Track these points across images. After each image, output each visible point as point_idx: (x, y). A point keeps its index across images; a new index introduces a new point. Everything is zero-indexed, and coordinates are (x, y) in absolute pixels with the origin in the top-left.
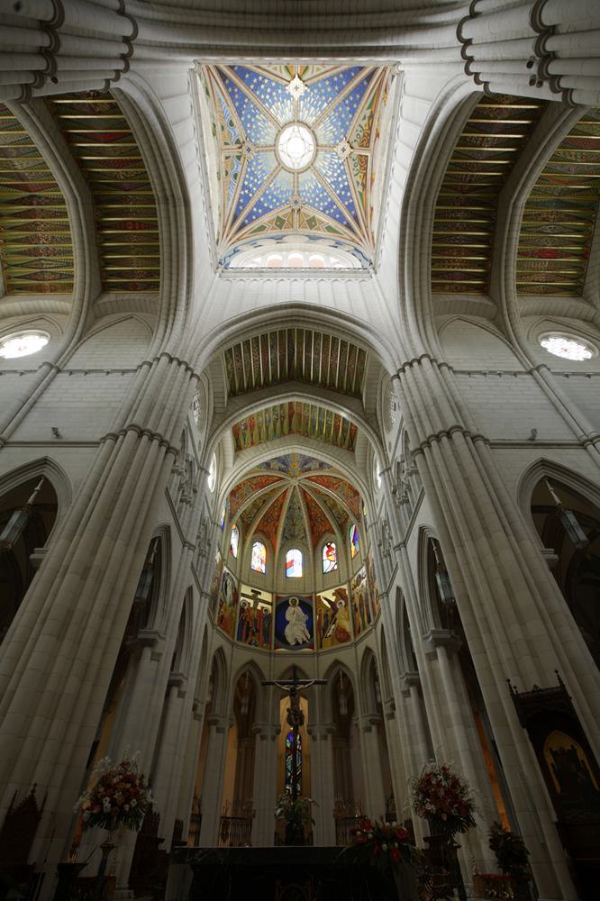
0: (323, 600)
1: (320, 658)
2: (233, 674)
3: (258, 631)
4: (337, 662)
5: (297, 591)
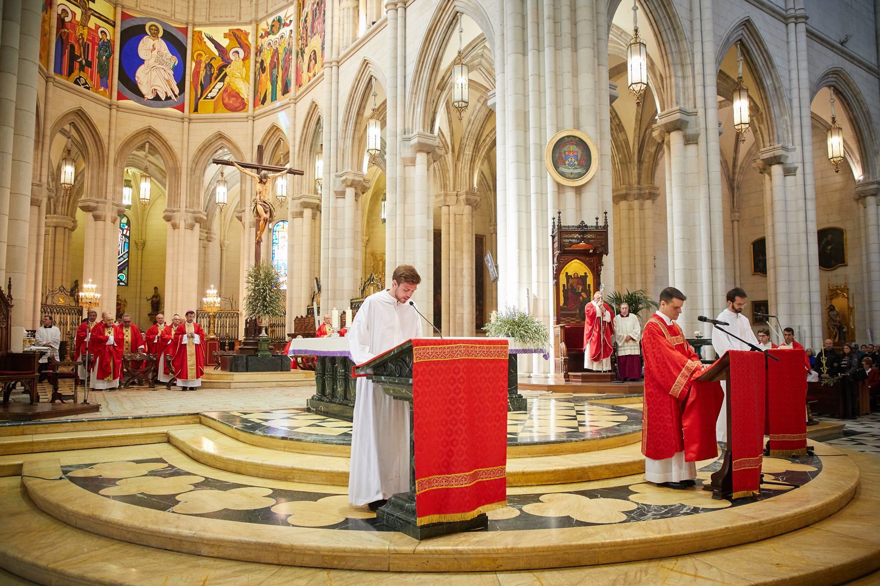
0: (206, 40)
3: (89, 64)
5: (163, 13)
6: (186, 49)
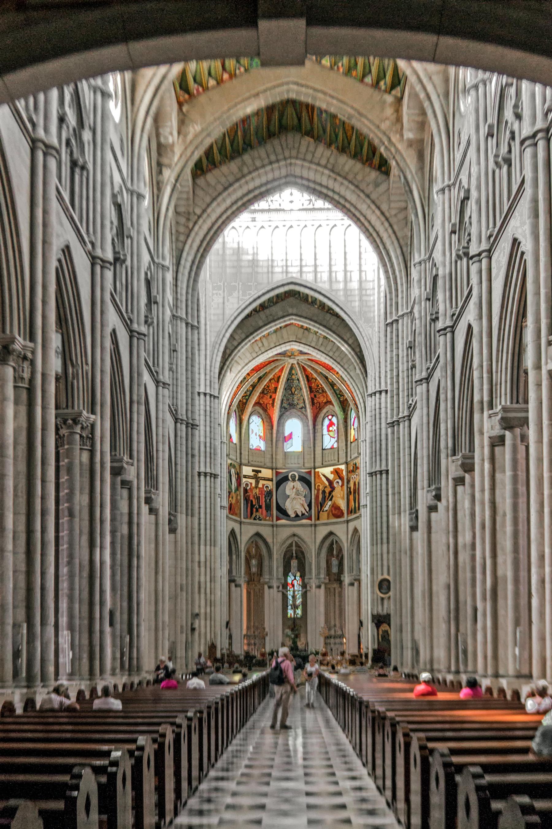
0: (322, 476)
1: (318, 528)
2: (243, 546)
3: (260, 507)
4: (331, 533)
6: (311, 483)
